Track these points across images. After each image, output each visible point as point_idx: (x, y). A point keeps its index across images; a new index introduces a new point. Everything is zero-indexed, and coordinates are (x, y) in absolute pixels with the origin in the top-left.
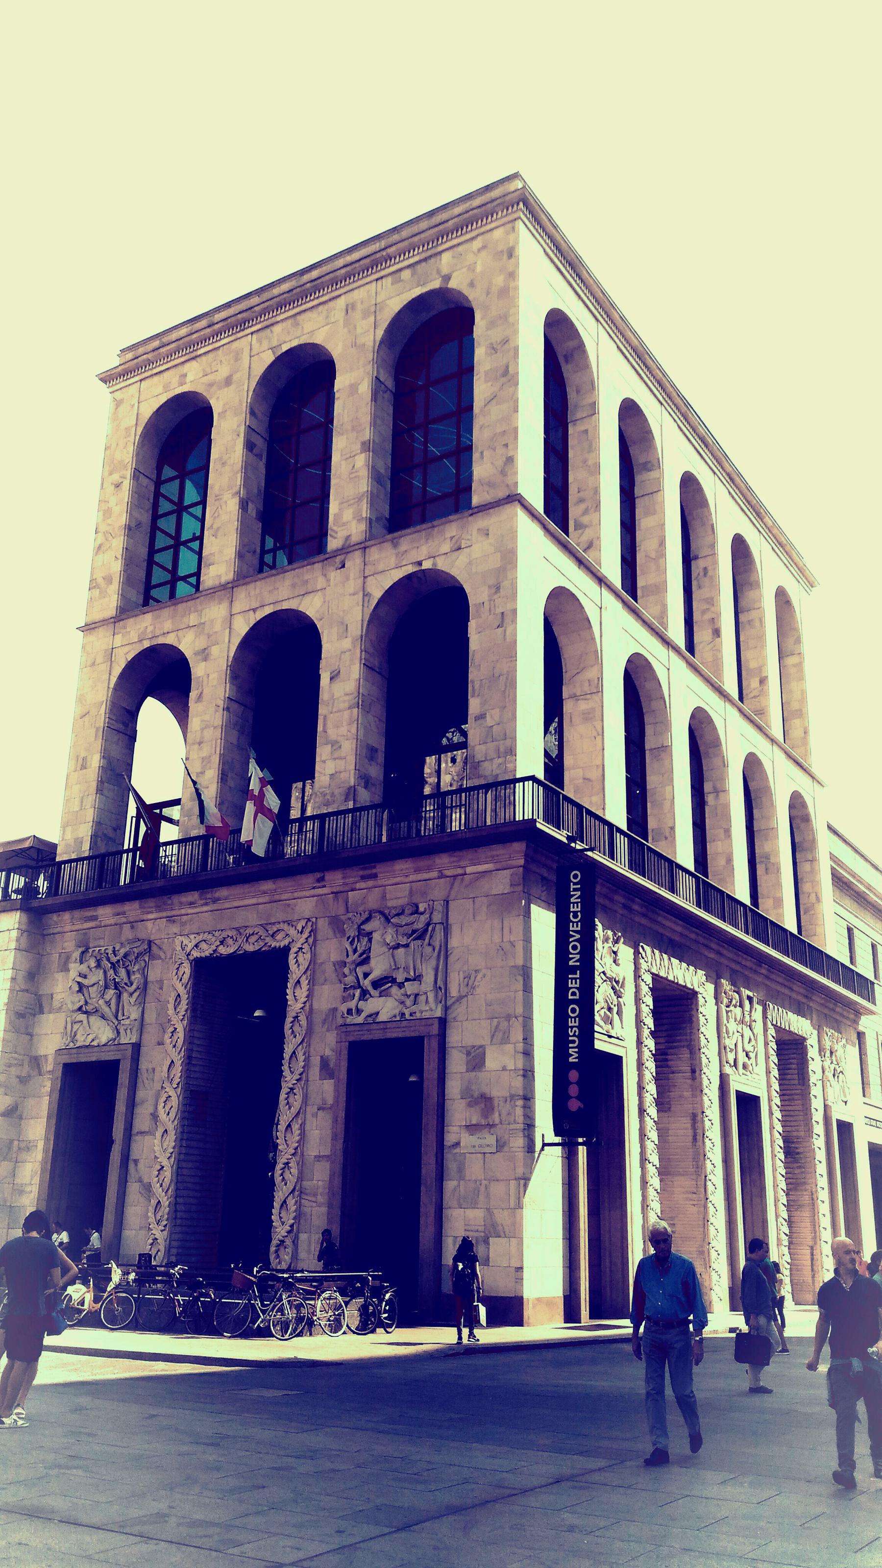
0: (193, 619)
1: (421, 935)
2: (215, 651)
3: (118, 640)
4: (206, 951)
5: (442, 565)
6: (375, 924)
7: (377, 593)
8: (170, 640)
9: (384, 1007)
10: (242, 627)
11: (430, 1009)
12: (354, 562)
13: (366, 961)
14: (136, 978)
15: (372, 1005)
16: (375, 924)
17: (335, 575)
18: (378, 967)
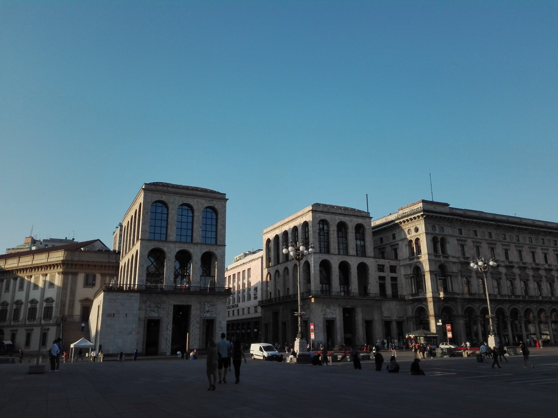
0: (167, 245)
1: (213, 306)
2: (172, 252)
3: (149, 244)
4: (176, 304)
5: (214, 251)
6: (206, 303)
7: (203, 252)
8: (162, 247)
9: (208, 315)
10: (178, 250)
11: (214, 315)
12: (199, 246)
13: (204, 308)
14: (162, 307)
15: (205, 315)
16: (206, 303)
17: (196, 247)
18: (207, 309)
